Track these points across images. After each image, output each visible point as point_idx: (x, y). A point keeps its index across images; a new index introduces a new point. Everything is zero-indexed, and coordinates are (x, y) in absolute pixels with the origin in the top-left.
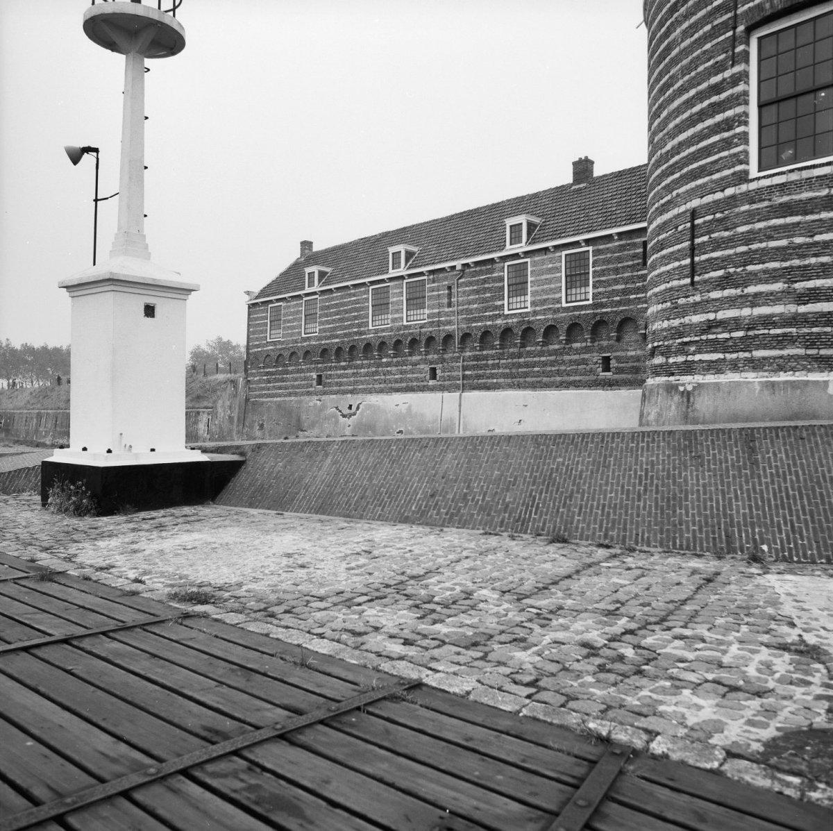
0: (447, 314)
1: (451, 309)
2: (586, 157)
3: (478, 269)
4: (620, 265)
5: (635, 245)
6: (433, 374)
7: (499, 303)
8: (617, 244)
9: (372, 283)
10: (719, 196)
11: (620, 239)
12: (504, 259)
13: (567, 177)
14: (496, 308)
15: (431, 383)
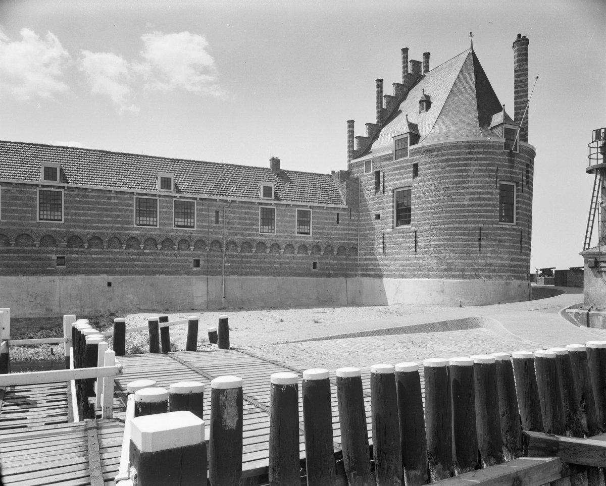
0: (214, 228)
1: (219, 225)
2: (279, 160)
3: (241, 205)
4: (326, 221)
5: (333, 214)
6: (197, 263)
7: (256, 227)
8: (325, 211)
9: (138, 194)
10: (490, 226)
11: (326, 210)
12: (260, 204)
13: (267, 165)
14: (253, 229)
15: (195, 269)
